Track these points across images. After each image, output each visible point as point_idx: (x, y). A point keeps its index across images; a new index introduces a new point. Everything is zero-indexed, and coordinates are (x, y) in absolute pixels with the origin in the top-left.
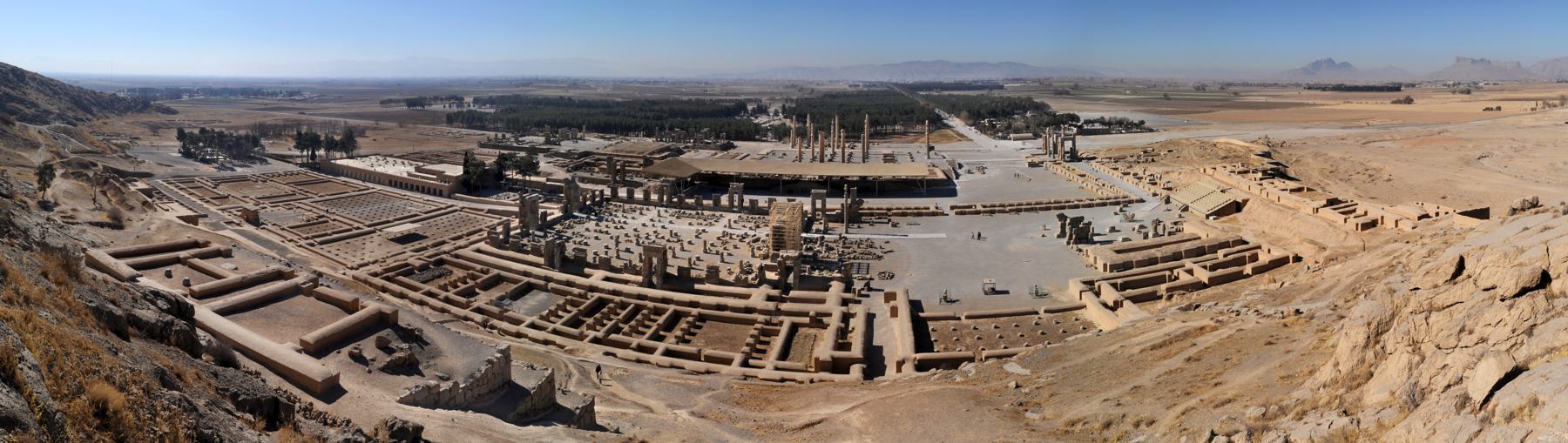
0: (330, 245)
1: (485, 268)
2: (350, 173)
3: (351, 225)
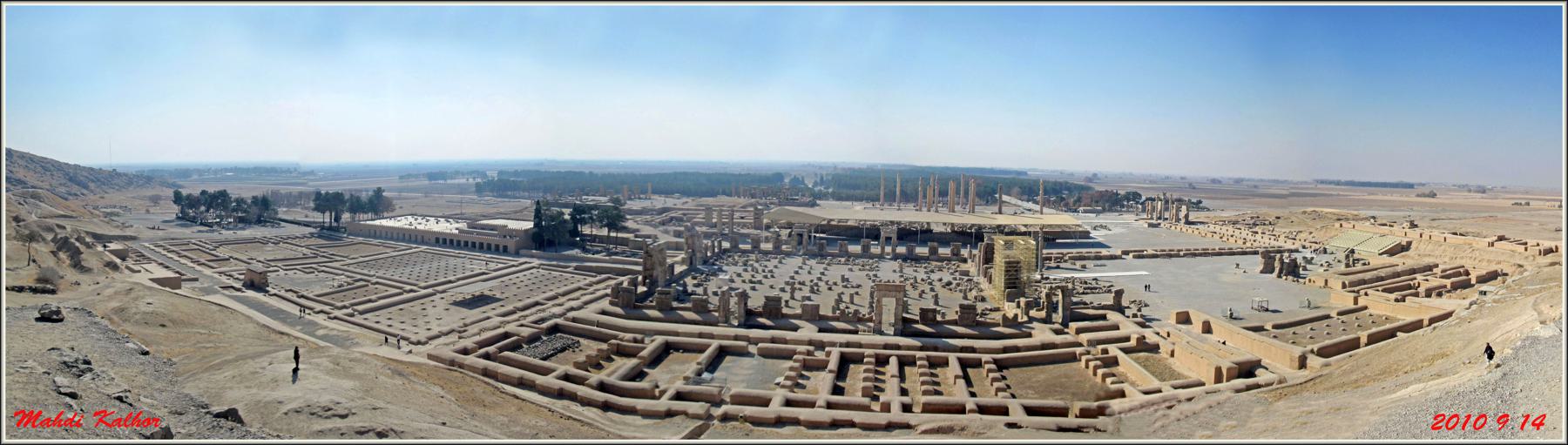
0: (377, 313)
1: (639, 336)
2: (395, 235)
3: (400, 288)
